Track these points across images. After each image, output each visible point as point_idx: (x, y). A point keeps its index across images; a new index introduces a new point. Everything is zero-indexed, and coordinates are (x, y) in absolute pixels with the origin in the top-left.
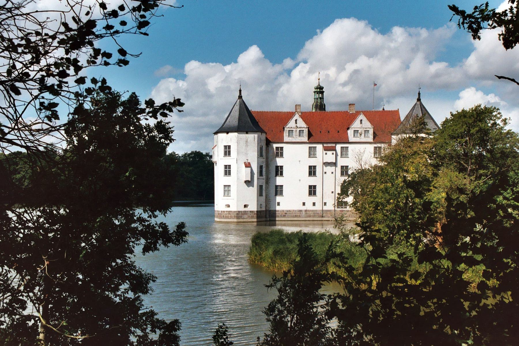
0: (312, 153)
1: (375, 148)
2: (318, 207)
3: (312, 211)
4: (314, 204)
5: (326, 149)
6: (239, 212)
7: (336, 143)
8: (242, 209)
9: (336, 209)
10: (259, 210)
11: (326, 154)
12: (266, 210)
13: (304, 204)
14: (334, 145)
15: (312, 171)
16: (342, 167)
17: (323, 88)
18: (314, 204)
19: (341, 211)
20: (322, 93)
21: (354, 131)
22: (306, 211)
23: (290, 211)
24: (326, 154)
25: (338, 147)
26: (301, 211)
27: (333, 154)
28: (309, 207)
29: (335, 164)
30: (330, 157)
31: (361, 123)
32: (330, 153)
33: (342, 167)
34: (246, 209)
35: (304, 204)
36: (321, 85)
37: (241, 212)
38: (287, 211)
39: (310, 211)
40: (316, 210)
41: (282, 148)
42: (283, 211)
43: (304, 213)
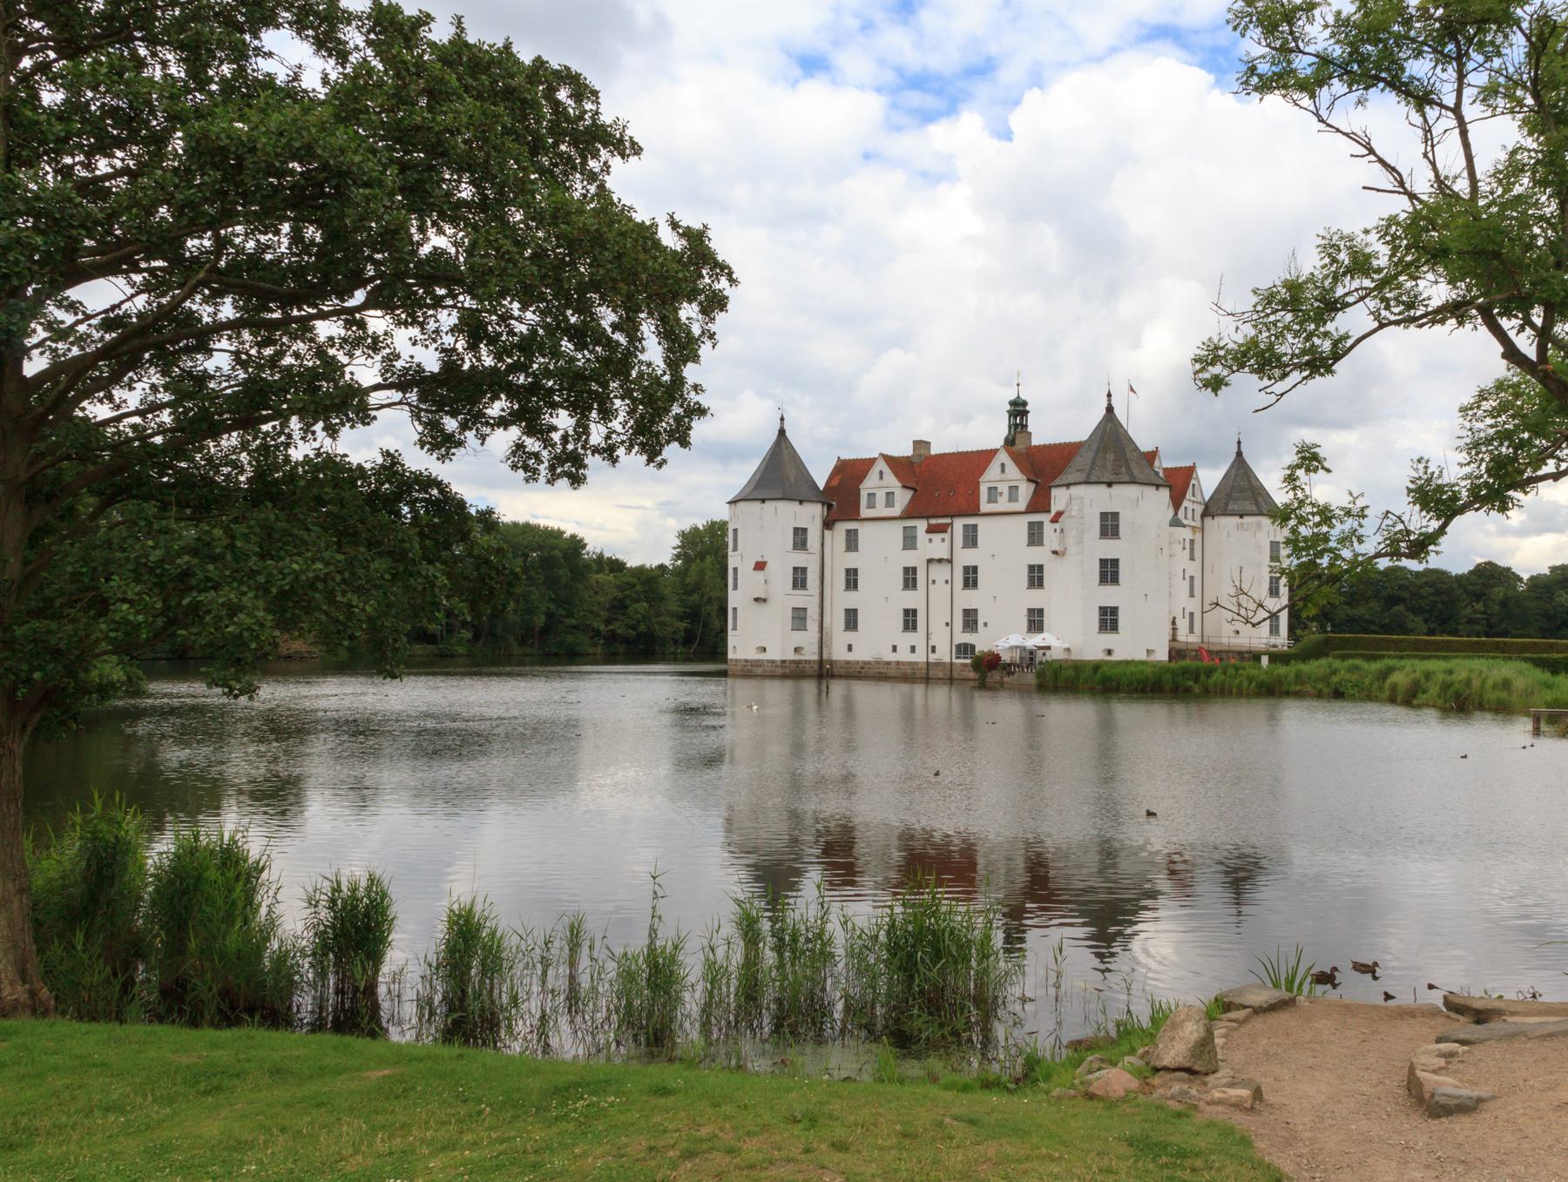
0: (910, 542)
1: (1031, 524)
2: (920, 657)
3: (910, 663)
4: (913, 649)
5: (931, 530)
6: (746, 661)
7: (952, 516)
8: (753, 655)
9: (954, 661)
10: (791, 656)
11: (931, 540)
12: (821, 662)
13: (894, 649)
14: (948, 521)
15: (910, 578)
16: (966, 569)
17: (1025, 404)
18: (913, 649)
19: (962, 665)
20: (1025, 413)
21: (990, 489)
22: (898, 663)
23: (869, 663)
24: (931, 540)
25: (959, 524)
26: (889, 663)
27: (943, 540)
28: (904, 655)
29: (950, 561)
30: (937, 546)
31: (1003, 470)
32: (937, 537)
33: (966, 569)
34: (762, 656)
35: (894, 649)
36: (1023, 397)
37: (751, 661)
38: (865, 663)
39: (904, 663)
40: (917, 663)
41: (856, 531)
42: (858, 662)
43: (893, 666)
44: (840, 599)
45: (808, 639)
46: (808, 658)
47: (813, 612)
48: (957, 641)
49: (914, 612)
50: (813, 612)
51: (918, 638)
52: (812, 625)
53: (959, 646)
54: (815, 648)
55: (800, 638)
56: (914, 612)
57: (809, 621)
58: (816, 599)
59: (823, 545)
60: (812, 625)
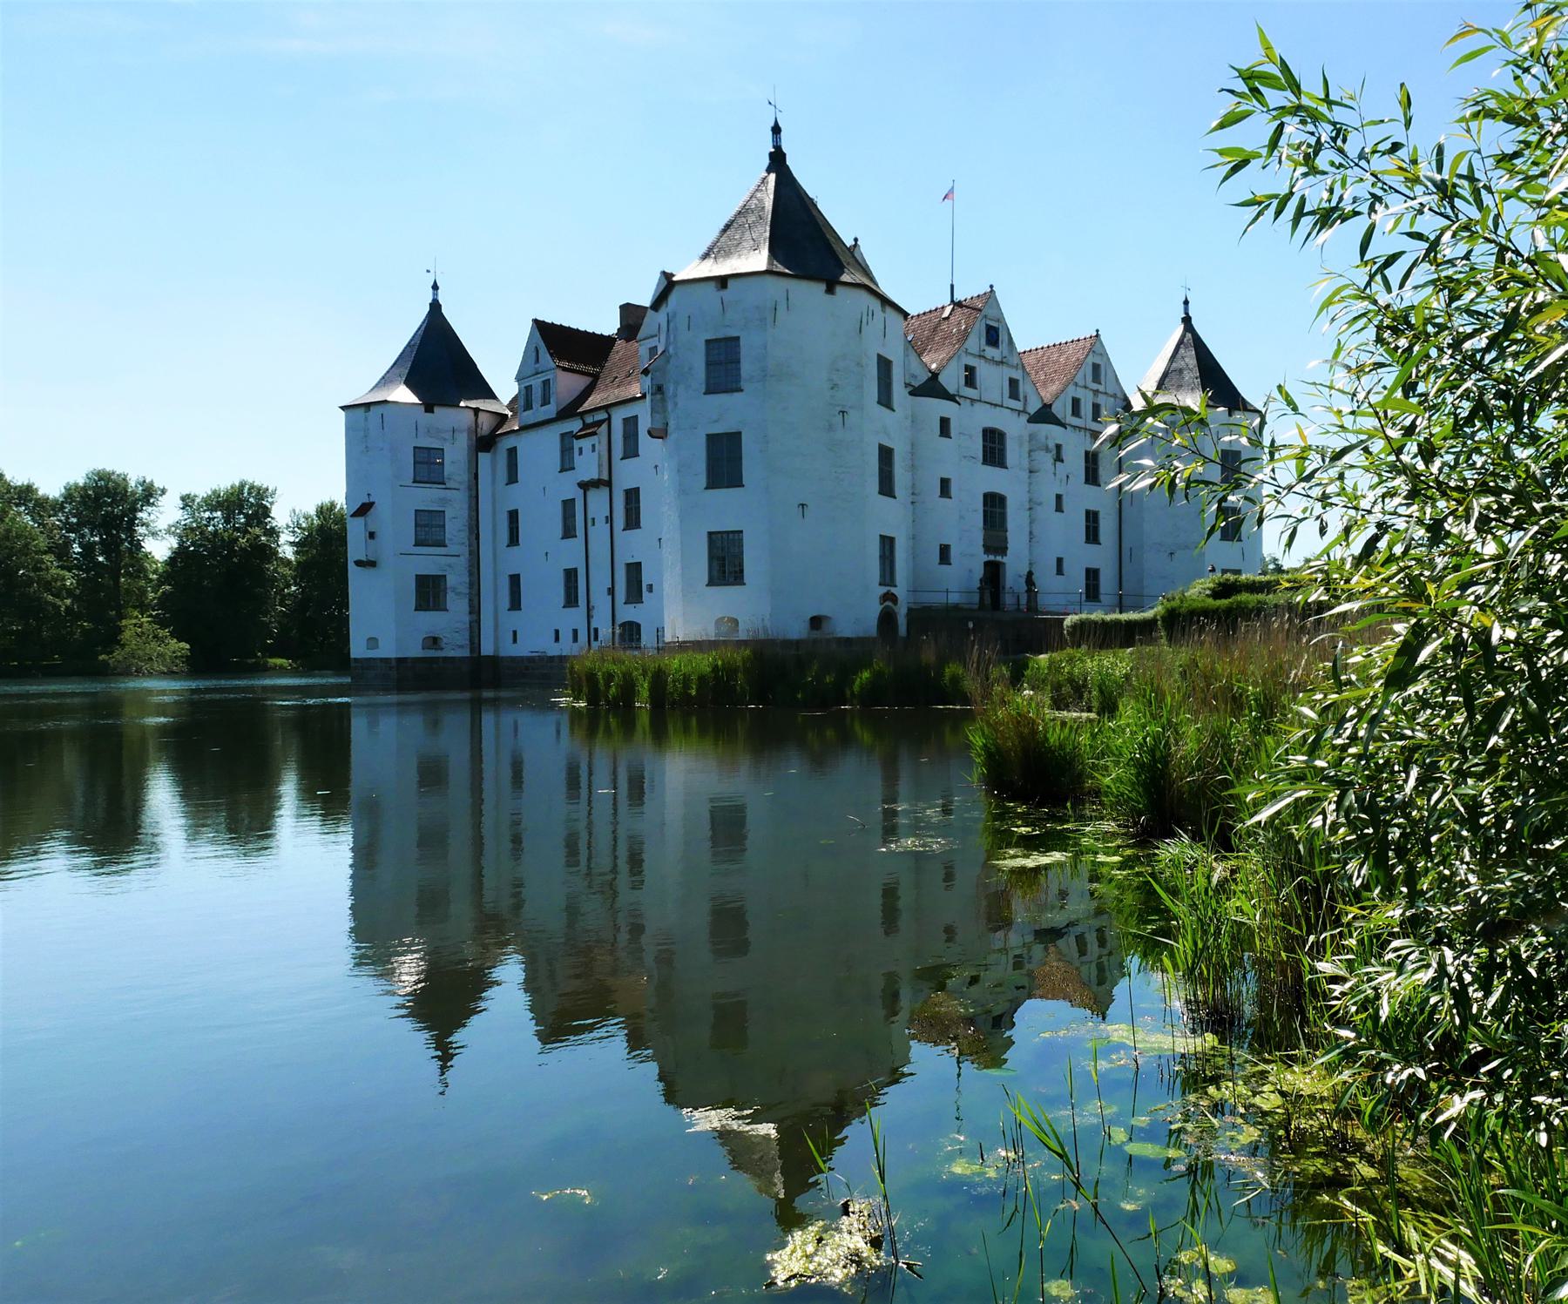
44: (497, 561)
45: (449, 623)
46: (452, 654)
47: (456, 579)
48: (619, 621)
49: (575, 570)
50: (456, 579)
51: (576, 617)
52: (457, 606)
53: (623, 625)
54: (463, 638)
55: (431, 622)
56: (575, 570)
57: (450, 596)
58: (462, 562)
59: (476, 476)
60: (457, 606)
